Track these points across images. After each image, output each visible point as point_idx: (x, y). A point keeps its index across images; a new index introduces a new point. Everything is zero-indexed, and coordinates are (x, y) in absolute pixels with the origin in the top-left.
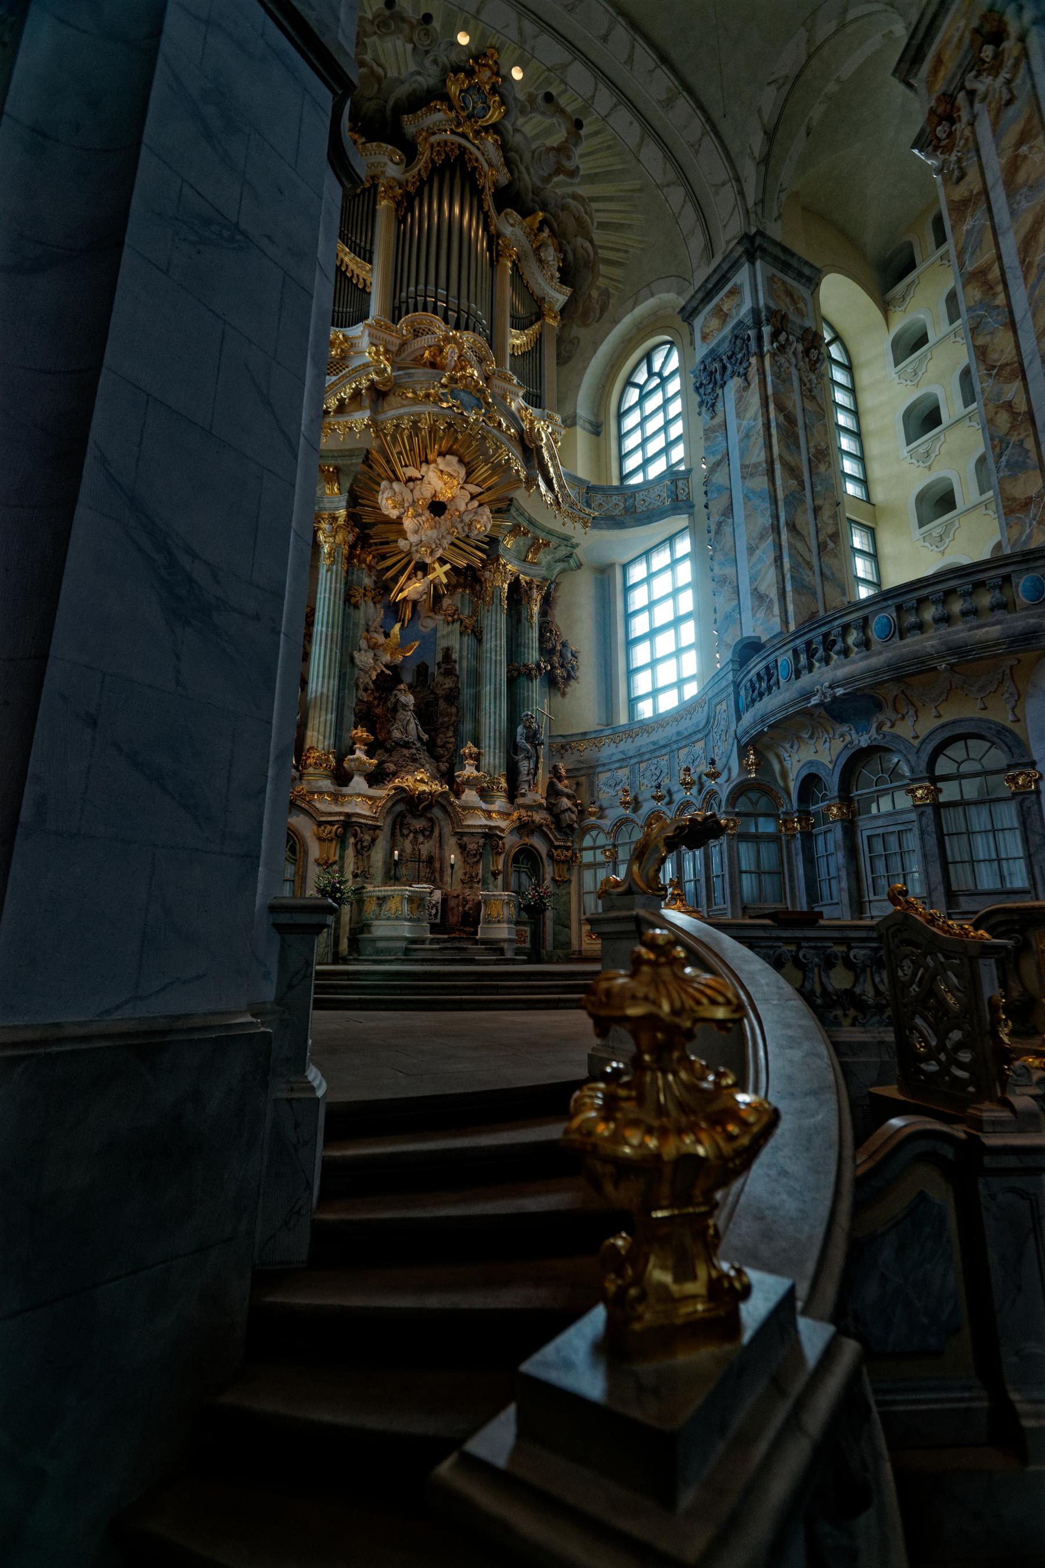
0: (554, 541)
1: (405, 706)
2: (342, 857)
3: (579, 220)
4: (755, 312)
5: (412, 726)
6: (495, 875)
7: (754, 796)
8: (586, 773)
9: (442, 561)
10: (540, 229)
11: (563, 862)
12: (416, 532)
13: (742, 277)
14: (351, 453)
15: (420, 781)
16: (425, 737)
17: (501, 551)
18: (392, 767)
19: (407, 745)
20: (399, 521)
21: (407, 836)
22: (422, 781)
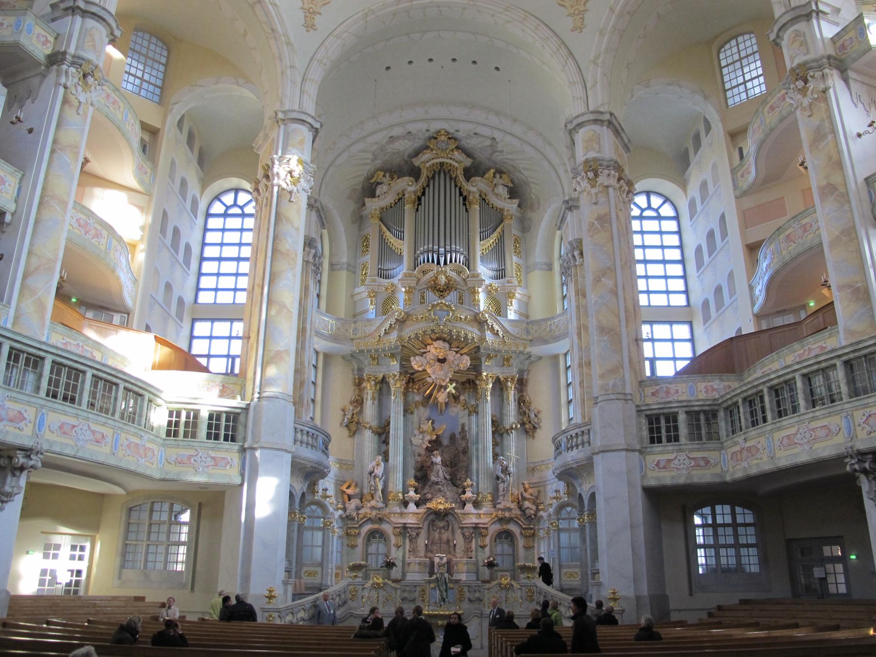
0: (513, 356)
1: (436, 464)
2: (404, 543)
3: (513, 166)
4: (570, 243)
5: (441, 472)
6: (483, 547)
7: (569, 509)
8: (540, 486)
9: (451, 381)
10: (494, 177)
11: (529, 537)
12: (434, 373)
13: (569, 219)
14: (396, 347)
15: (439, 503)
16: (448, 477)
17: (483, 367)
18: (429, 496)
19: (437, 483)
20: (424, 370)
21: (435, 531)
22: (440, 503)
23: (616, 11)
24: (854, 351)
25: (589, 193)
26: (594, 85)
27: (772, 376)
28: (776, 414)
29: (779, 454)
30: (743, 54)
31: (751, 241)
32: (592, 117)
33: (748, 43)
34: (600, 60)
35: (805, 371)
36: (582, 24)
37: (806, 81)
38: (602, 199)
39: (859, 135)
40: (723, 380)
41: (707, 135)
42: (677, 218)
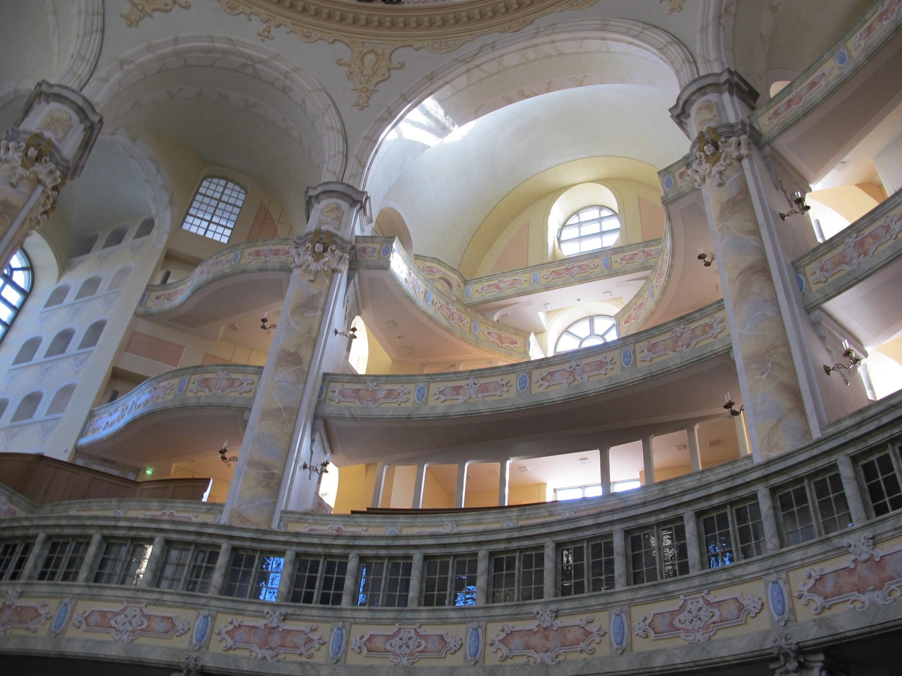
23: (178, 47)
24: (253, 540)
25: (13, 168)
26: (105, 80)
27: (122, 524)
28: (93, 576)
29: (72, 633)
30: (225, 198)
31: (123, 366)
32: (80, 102)
33: (235, 194)
34: (128, 67)
35: (174, 536)
36: (137, 22)
37: (325, 250)
38: (24, 188)
39: (336, 332)
40: (11, 502)
41: (135, 237)
42: (26, 294)
